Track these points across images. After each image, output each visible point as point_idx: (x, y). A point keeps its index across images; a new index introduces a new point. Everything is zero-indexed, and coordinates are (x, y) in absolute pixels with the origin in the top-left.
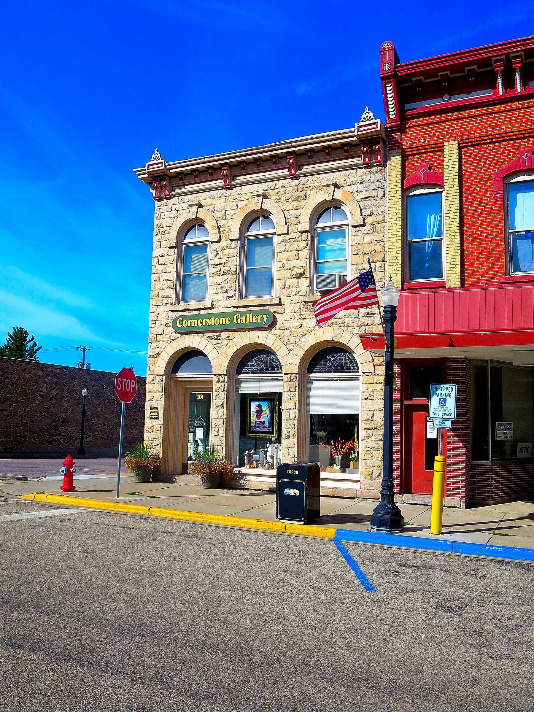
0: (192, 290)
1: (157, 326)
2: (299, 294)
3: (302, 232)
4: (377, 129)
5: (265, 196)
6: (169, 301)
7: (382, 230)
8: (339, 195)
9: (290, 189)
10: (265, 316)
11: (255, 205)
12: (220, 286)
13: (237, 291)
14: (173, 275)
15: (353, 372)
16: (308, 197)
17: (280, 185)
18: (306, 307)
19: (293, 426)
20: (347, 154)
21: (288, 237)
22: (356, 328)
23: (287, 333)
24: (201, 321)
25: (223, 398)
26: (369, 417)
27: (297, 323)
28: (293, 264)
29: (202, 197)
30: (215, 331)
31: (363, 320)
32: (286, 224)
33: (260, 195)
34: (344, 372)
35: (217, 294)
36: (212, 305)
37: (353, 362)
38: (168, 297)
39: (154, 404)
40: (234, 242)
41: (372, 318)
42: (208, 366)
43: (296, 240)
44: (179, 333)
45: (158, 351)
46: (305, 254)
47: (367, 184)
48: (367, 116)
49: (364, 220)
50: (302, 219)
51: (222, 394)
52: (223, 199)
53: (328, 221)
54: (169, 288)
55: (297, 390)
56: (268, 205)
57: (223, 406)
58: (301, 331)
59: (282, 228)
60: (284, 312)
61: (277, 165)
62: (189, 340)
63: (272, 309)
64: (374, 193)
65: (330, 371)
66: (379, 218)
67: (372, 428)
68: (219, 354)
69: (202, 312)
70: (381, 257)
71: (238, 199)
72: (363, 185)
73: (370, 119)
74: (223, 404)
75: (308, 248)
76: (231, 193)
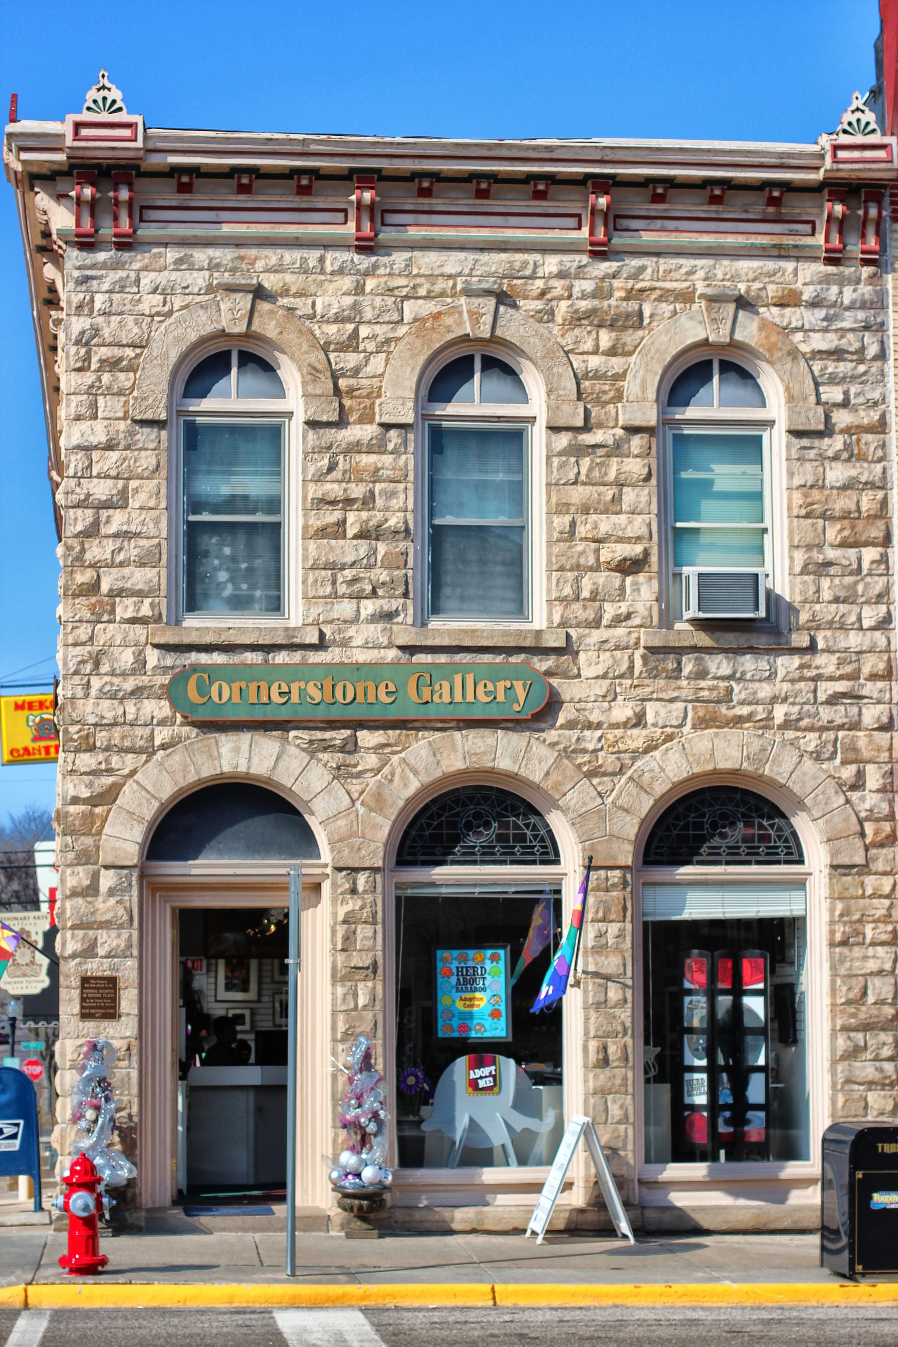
0: (223, 576)
1: (93, 692)
2: (629, 623)
3: (632, 430)
4: (888, 166)
5: (503, 298)
6: (145, 610)
7: (880, 453)
8: (748, 331)
9: (588, 286)
10: (519, 686)
11: (471, 319)
12: (348, 574)
13: (411, 595)
14: (157, 522)
15: (787, 862)
16: (646, 321)
17: (554, 269)
18: (652, 664)
19: (620, 1028)
20: (771, 209)
21: (588, 439)
22: (812, 736)
23: (591, 739)
24: (285, 689)
25: (369, 943)
26: (855, 993)
27: (622, 711)
28: (606, 524)
29: (266, 267)
30: (332, 725)
31: (826, 714)
32: (579, 398)
33: (488, 293)
34: (759, 863)
35: (328, 598)
36: (322, 635)
37: (787, 833)
38: (140, 594)
39: (96, 967)
40: (393, 433)
41: (855, 710)
42: (303, 841)
43: (617, 449)
44: (194, 724)
45: (108, 780)
46: (644, 499)
47: (832, 312)
48: (858, 121)
49: (828, 418)
50: (631, 386)
51: (368, 930)
52: (347, 283)
53: (712, 405)
54: (142, 565)
55: (628, 918)
56: (515, 326)
57: (375, 972)
58: (637, 738)
59: (566, 408)
60: (579, 676)
61: (544, 203)
62: (237, 750)
63: (542, 664)
64: (851, 342)
65: (737, 858)
66: (871, 417)
67: (866, 1027)
68: (351, 803)
69: (281, 658)
70: (876, 532)
71: (404, 292)
72: (821, 313)
73: (866, 130)
74: (375, 964)
75: (654, 481)
76: (375, 267)
